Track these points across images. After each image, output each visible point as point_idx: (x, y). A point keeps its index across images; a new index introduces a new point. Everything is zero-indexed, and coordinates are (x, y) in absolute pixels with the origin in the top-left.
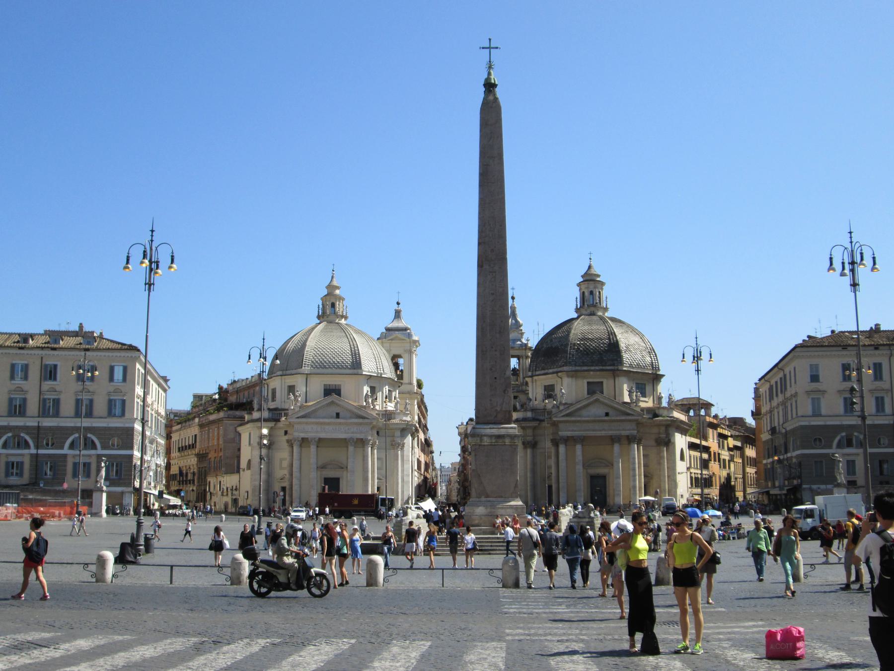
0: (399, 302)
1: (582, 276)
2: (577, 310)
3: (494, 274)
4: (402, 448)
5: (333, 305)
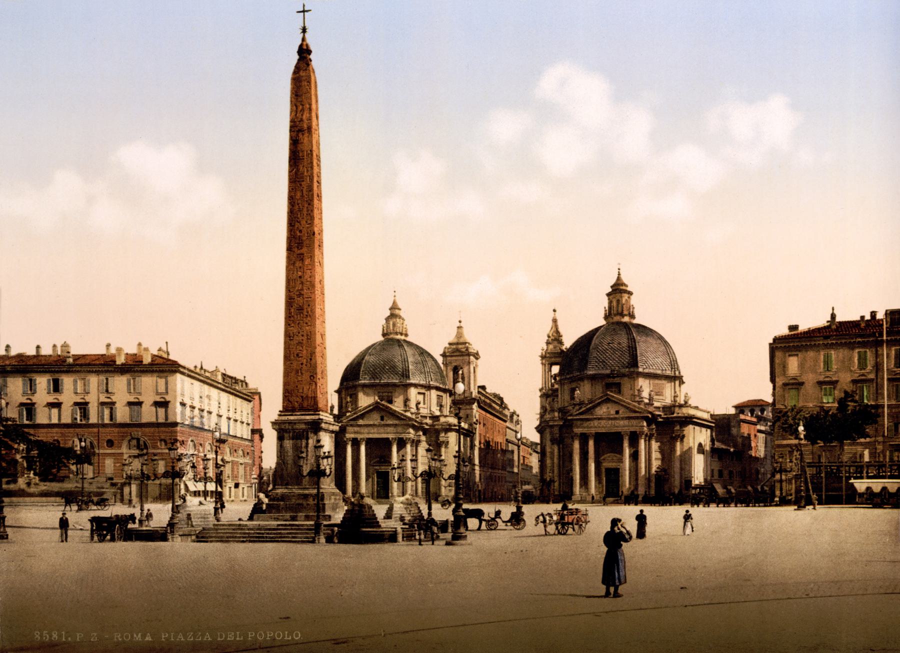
0: (462, 320)
1: (612, 287)
2: (606, 317)
3: (302, 256)
4: (446, 447)
5: (394, 325)
